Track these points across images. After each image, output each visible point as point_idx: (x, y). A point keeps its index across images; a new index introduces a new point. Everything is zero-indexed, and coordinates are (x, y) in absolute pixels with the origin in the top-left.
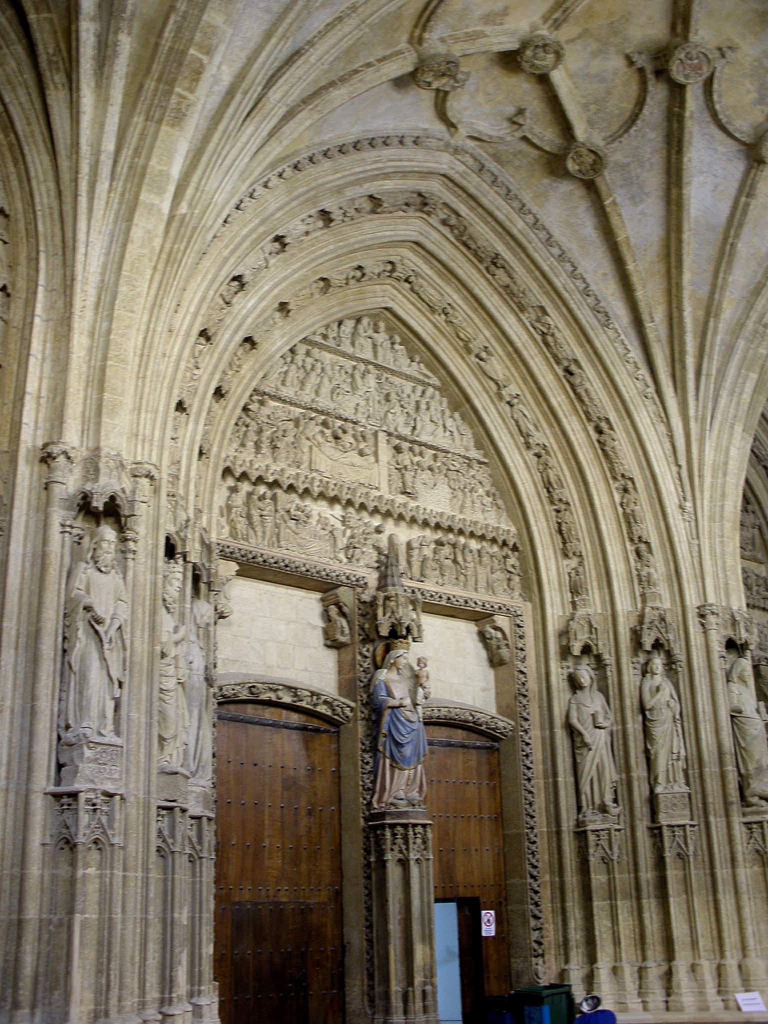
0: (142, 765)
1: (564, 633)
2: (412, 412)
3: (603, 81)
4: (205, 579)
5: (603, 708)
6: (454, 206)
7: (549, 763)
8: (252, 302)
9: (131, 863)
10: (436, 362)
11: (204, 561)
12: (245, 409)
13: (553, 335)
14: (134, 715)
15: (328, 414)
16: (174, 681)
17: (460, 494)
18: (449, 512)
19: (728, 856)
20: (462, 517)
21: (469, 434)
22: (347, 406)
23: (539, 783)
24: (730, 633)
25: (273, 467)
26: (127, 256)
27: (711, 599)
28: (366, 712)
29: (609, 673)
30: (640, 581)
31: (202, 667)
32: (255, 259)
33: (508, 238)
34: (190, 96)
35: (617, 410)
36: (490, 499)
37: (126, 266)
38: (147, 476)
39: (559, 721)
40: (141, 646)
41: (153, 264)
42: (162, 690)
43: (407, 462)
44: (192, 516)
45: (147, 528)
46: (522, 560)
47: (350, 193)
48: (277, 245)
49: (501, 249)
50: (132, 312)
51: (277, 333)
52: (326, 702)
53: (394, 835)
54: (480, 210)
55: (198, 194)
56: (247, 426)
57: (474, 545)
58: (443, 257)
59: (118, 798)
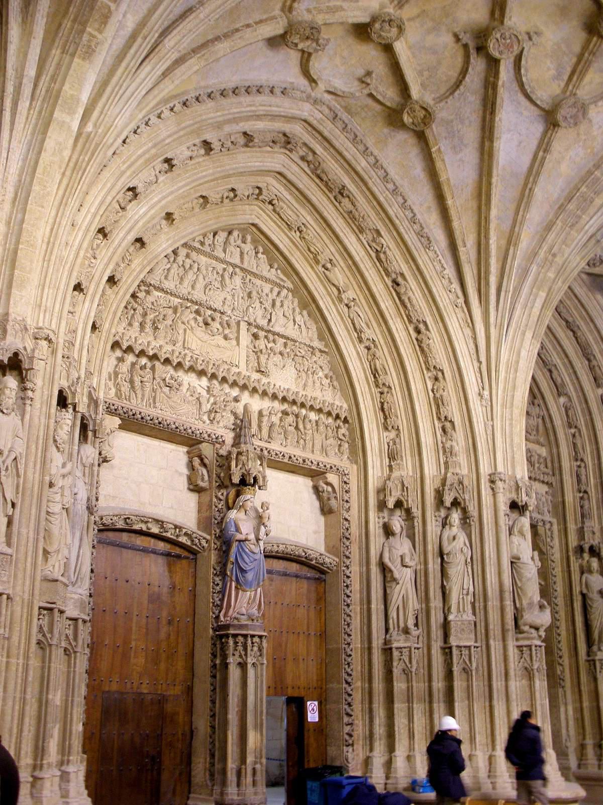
0: (28, 572)
1: (382, 490)
2: (269, 308)
3: (435, 52)
4: (91, 427)
5: (410, 550)
6: (312, 146)
7: (365, 593)
8: (144, 209)
9: (14, 651)
10: (290, 269)
11: (92, 413)
12: (134, 296)
13: (385, 253)
14: (24, 531)
15: (201, 304)
16: (60, 506)
17: (304, 374)
18: (294, 388)
19: (503, 672)
20: (304, 393)
21: (314, 327)
22: (216, 299)
23: (356, 609)
24: (514, 496)
25: (153, 344)
26: (41, 161)
27: (500, 468)
28: (218, 543)
29: (416, 524)
30: (445, 452)
31: (85, 499)
32: (147, 175)
33: (353, 173)
34: (99, 36)
35: (433, 315)
36: (328, 381)
37: (40, 170)
38: (46, 339)
39: (374, 560)
40: (33, 476)
41: (62, 170)
42: (48, 513)
43: (262, 347)
44: (83, 376)
45: (44, 381)
46: (351, 431)
47: (227, 129)
48: (166, 165)
49: (347, 182)
50: (43, 207)
51: (163, 237)
52: (186, 534)
53: (236, 643)
54: (331, 150)
55: (102, 117)
56: (134, 310)
57: (313, 416)
58: (301, 186)
59: (5, 597)
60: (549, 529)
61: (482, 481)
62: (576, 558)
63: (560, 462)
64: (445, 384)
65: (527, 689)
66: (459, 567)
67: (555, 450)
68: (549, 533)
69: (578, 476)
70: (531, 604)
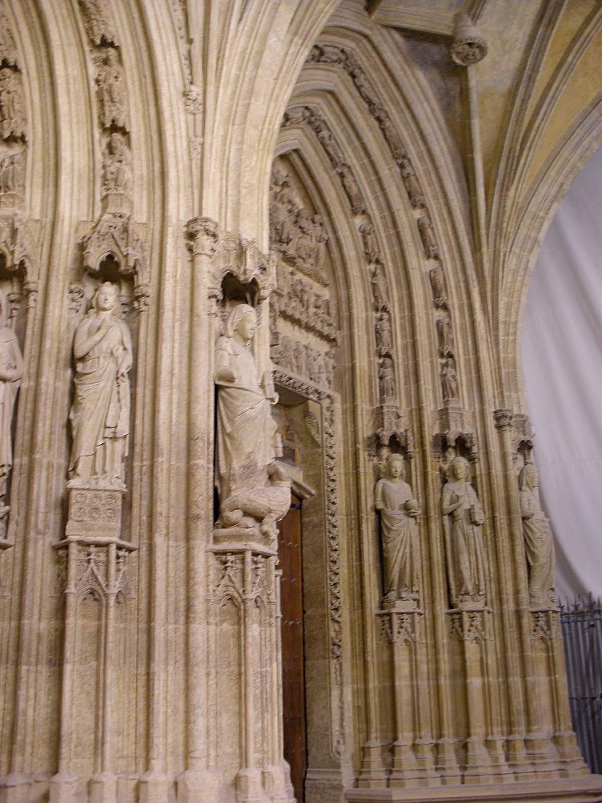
19: (182, 604)
24: (233, 265)
60: (328, 409)
61: (170, 231)
62: (370, 455)
63: (350, 309)
64: (120, 69)
65: (232, 642)
66: (102, 384)
67: (343, 293)
68: (327, 414)
69: (378, 333)
70: (250, 469)
